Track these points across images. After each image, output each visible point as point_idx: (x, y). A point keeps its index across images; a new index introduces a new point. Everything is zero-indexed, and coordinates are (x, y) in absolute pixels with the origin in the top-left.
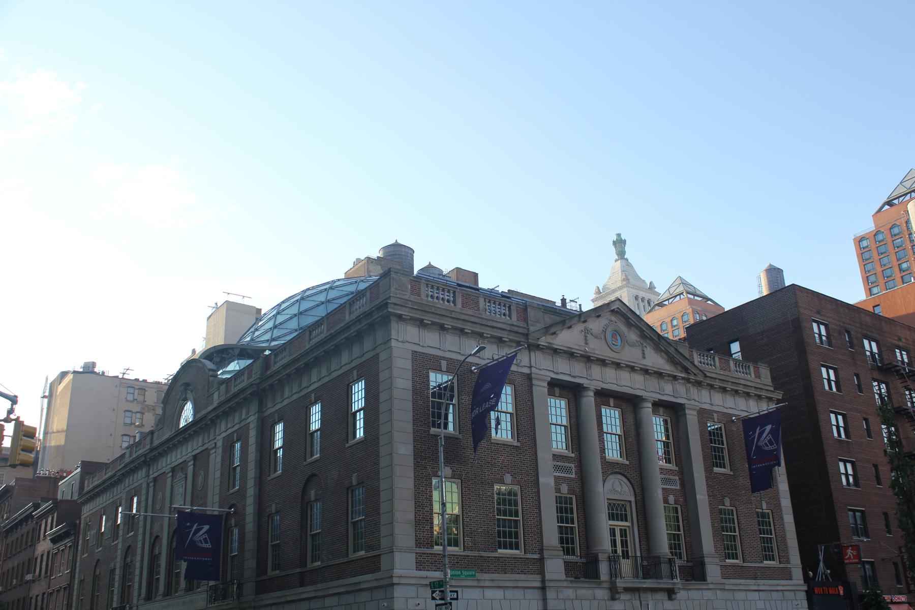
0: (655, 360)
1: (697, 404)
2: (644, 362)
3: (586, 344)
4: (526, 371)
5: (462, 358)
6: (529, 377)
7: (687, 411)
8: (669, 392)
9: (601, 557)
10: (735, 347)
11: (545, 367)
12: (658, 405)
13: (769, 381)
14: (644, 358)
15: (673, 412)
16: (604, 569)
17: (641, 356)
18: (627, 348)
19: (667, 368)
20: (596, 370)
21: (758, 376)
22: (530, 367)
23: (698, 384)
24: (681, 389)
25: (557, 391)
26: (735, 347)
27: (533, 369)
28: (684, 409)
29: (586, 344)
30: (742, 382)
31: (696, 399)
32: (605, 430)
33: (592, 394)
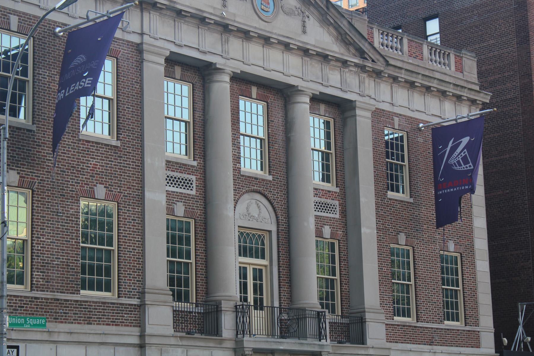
0: (319, 36)
1: (372, 102)
2: (305, 38)
3: (224, 6)
4: (136, 39)
5: (40, 14)
6: (139, 49)
7: (358, 112)
8: (335, 82)
9: (225, 305)
10: (433, 27)
11: (161, 35)
12: (317, 100)
13: (473, 77)
14: (304, 32)
15: (338, 110)
16: (227, 321)
17: (300, 30)
18: (282, 16)
19: (335, 48)
20: (235, 46)
21: (460, 68)
22: (142, 34)
23: (377, 74)
24: (352, 79)
25: (178, 71)
26: (433, 27)
27: (145, 37)
28: (354, 108)
29: (224, 6)
30: (438, 76)
31: (371, 96)
32: (242, 131)
33: (227, 79)
